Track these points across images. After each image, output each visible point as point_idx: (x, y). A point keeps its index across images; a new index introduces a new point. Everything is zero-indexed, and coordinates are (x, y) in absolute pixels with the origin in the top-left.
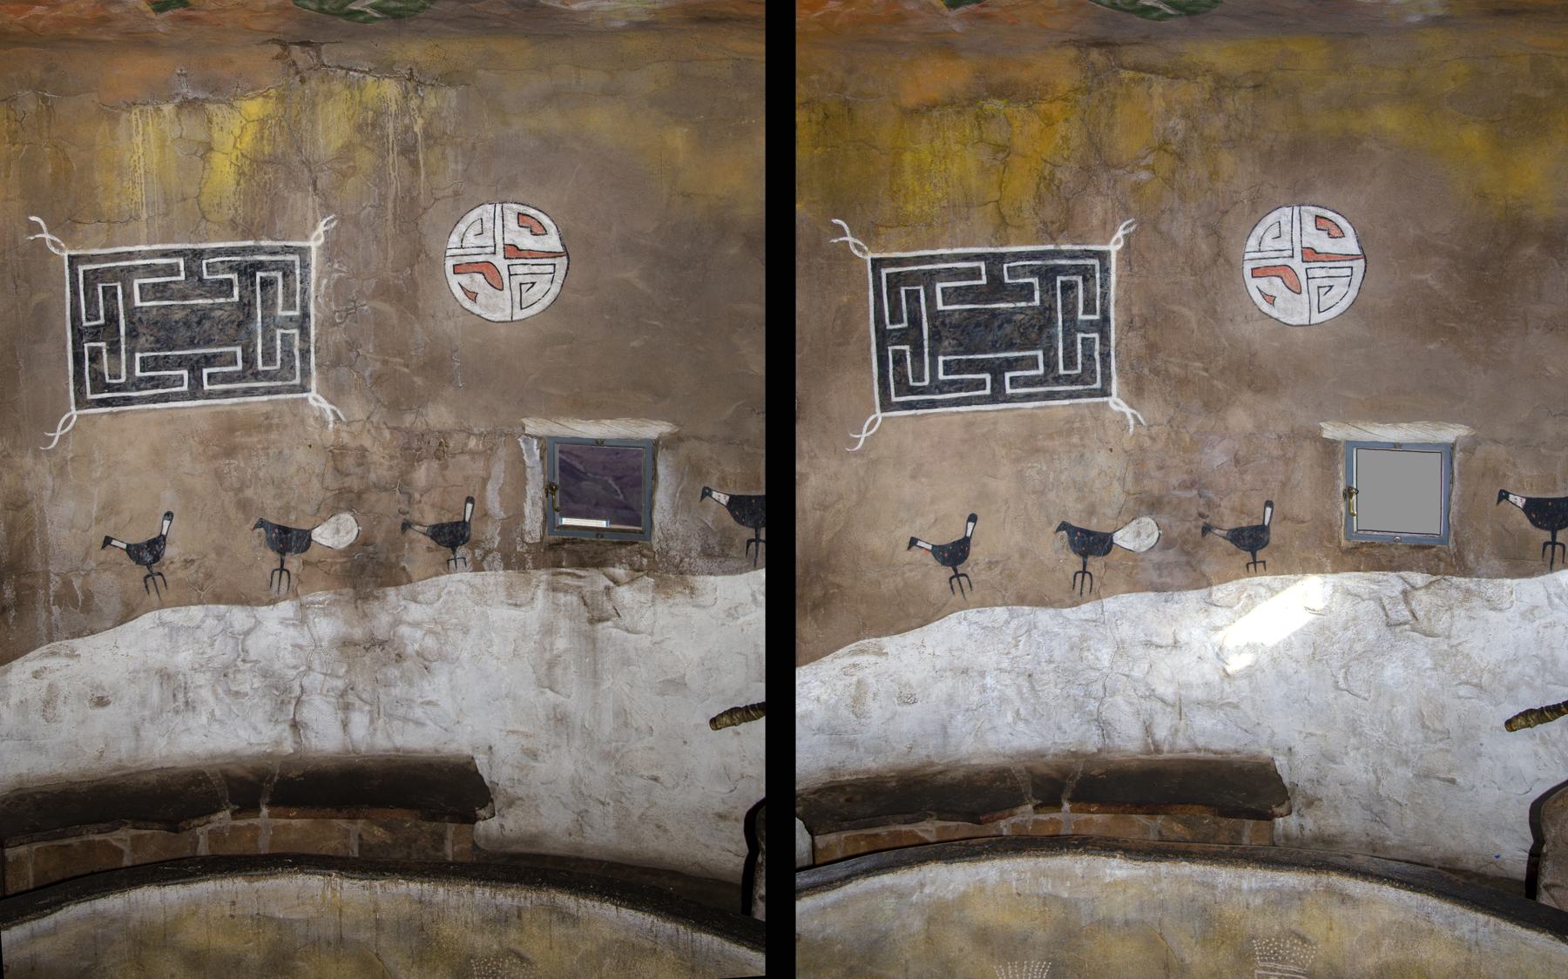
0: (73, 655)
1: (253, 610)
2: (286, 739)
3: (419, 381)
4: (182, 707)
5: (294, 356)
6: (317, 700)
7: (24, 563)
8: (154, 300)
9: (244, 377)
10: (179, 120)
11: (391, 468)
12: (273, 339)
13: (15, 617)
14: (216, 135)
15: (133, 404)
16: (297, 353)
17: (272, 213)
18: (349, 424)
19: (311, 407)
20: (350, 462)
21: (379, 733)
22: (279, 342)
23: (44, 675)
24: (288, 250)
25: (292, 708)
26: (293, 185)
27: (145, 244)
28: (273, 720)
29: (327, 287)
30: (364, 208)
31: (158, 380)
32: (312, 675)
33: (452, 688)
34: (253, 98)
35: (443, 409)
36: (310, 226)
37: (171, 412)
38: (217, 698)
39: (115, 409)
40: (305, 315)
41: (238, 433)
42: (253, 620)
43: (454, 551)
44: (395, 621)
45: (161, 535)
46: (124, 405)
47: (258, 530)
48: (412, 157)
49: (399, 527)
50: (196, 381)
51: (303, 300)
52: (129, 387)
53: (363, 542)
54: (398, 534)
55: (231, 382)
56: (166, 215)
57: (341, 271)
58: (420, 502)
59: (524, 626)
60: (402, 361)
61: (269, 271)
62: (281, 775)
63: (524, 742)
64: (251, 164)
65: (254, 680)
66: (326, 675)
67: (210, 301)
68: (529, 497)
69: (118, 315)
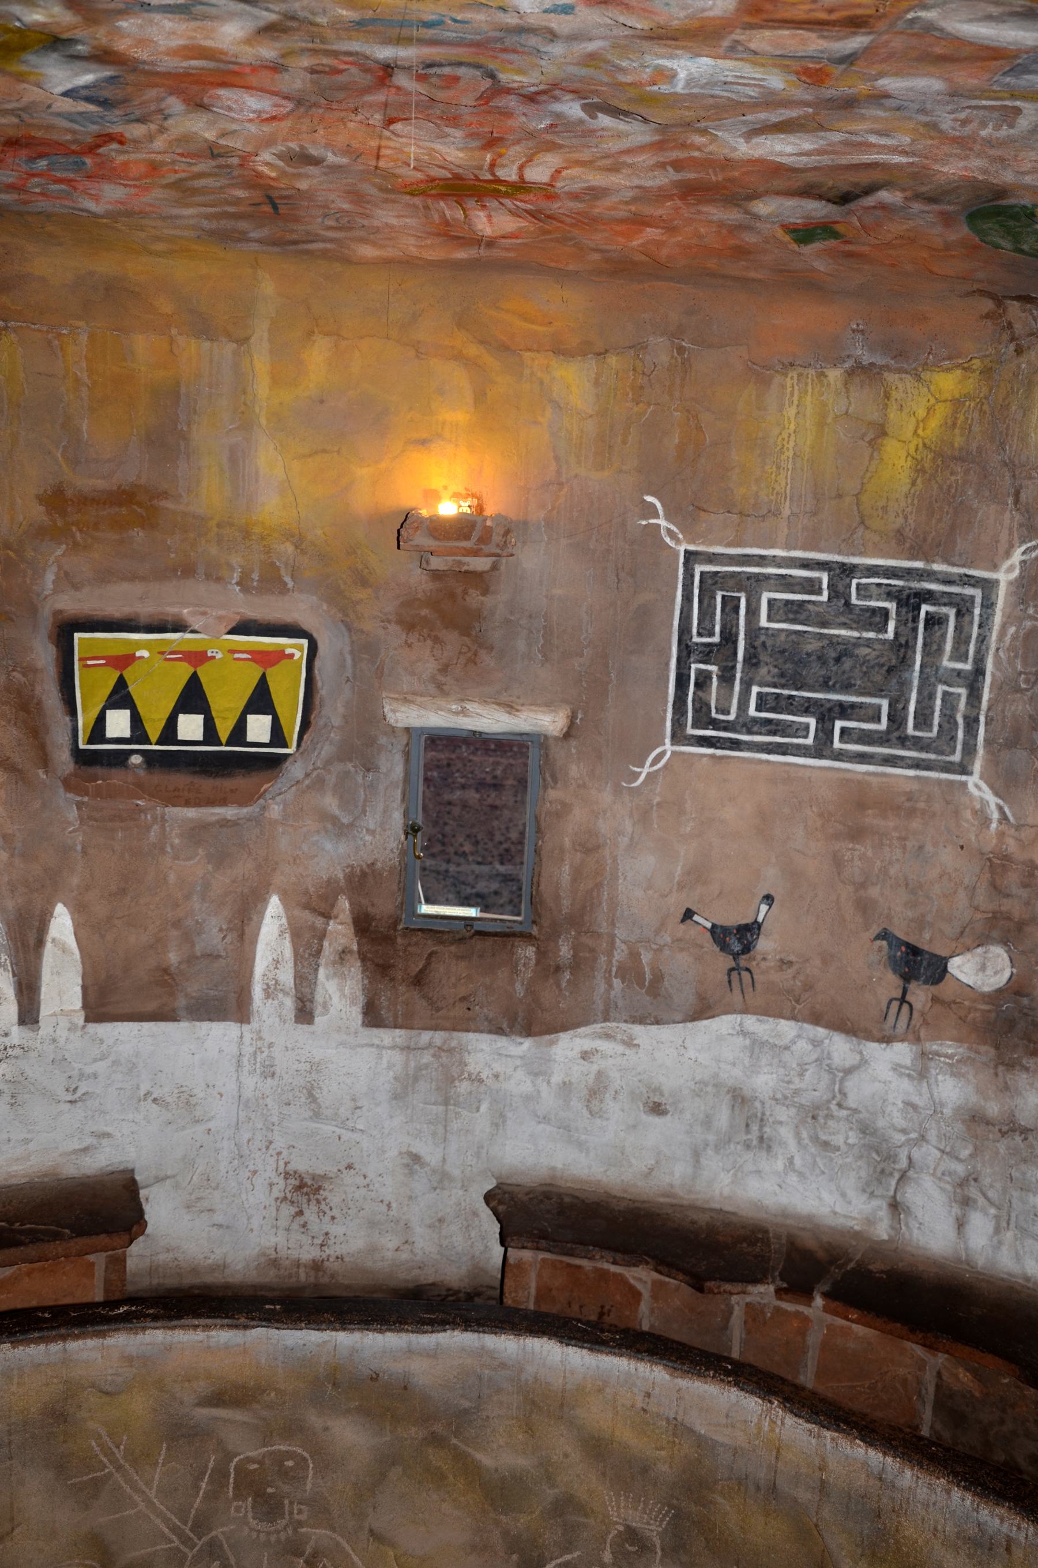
0: (630, 1043)
1: (859, 1044)
2: (881, 1220)
4: (755, 1143)
5: (956, 723)
6: (928, 1183)
7: (586, 918)
9: (888, 741)
10: (847, 391)
12: (932, 696)
13: (569, 981)
14: (893, 415)
15: (741, 750)
16: (960, 720)
18: (1018, 828)
21: (1005, 1249)
22: (938, 702)
23: (594, 1059)
24: (967, 580)
25: (893, 1182)
26: (987, 494)
27: (783, 548)
28: (867, 1190)
29: (1014, 638)
31: (777, 725)
32: (925, 1148)
34: (948, 370)
36: (1001, 551)
37: (787, 768)
38: (799, 1143)
39: (719, 752)
40: (979, 671)
41: (870, 812)
42: (858, 1057)
45: (756, 921)
47: (878, 943)
50: (825, 734)
51: (978, 651)
52: (738, 728)
53: (1015, 989)
55: (869, 744)
61: (940, 605)
62: (859, 1264)
64: (934, 459)
65: (850, 1134)
66: (943, 1152)
67: (856, 634)
69: (737, 635)
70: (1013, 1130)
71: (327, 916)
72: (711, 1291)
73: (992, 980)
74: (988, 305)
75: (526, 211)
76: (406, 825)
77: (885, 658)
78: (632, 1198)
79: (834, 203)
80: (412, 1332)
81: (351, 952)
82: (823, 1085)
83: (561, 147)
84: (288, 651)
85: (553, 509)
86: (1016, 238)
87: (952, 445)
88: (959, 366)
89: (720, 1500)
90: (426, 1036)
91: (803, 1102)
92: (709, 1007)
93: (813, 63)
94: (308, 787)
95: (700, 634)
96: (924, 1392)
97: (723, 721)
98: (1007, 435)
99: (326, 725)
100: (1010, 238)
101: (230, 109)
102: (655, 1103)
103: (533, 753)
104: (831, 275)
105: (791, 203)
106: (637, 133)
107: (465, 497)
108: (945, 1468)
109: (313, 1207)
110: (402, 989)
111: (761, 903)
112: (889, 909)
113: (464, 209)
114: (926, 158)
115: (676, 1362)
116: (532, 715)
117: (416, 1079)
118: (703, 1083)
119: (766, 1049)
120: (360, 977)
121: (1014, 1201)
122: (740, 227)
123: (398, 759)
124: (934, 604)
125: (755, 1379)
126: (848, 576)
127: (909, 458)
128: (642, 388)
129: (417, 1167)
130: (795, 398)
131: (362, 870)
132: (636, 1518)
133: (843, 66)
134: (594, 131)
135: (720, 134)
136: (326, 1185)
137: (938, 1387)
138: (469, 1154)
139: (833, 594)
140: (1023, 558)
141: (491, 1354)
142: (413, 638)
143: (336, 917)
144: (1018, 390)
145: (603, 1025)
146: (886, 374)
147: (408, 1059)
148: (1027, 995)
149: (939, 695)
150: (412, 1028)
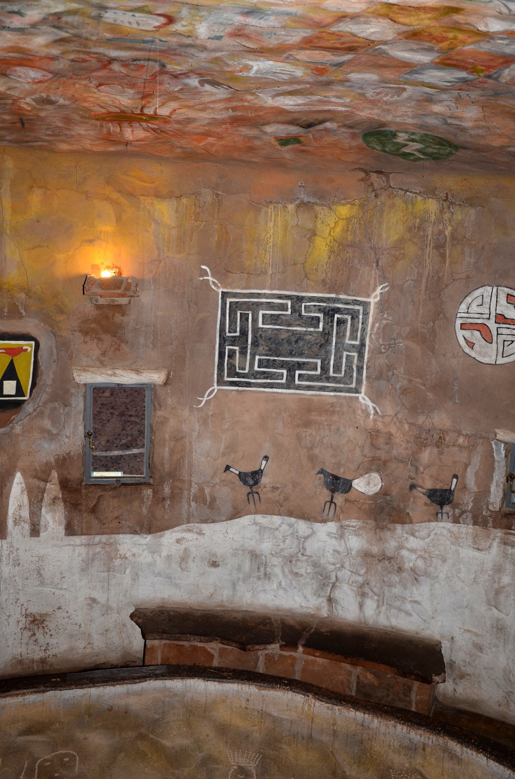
0: (200, 533)
2: (324, 607)
3: (430, 395)
4: (262, 576)
5: (353, 369)
6: (345, 587)
7: (177, 473)
8: (270, 324)
9: (321, 379)
10: (297, 214)
11: (406, 448)
12: (341, 357)
13: (169, 505)
16: (355, 368)
17: (348, 278)
19: (360, 403)
20: (381, 441)
21: (382, 615)
22: (344, 360)
23: (183, 542)
25: (329, 589)
26: (364, 262)
29: (378, 329)
30: (407, 281)
31: (268, 374)
32: (344, 571)
33: (432, 595)
34: (344, 205)
35: (444, 416)
36: (371, 288)
37: (274, 395)
38: (284, 574)
39: (241, 389)
40: (363, 345)
41: (313, 413)
42: (311, 531)
43: (442, 508)
44: (400, 546)
45: (260, 469)
46: (246, 387)
47: (319, 475)
48: (442, 251)
49: (408, 487)
50: (291, 377)
51: (362, 335)
53: (384, 493)
54: (407, 491)
55: (312, 381)
56: (284, 273)
57: (388, 320)
58: (423, 473)
59: (483, 564)
60: (421, 381)
61: (343, 314)
63: (474, 638)
65: (308, 568)
66: (352, 572)
67: (305, 329)
68: (495, 480)
69: (248, 331)
70: (384, 559)
71: (46, 481)
72: (249, 650)
73: (373, 489)
74: (362, 175)
75: (152, 129)
76: (85, 432)
77: (319, 340)
78: (203, 609)
79: (303, 127)
80: (129, 684)
81: (58, 498)
82: (294, 545)
83: (180, 99)
84: (25, 348)
85: (156, 273)
86: (383, 145)
87: (347, 239)
88: (349, 203)
89: (284, 746)
90: (97, 538)
91: (285, 554)
92: (239, 512)
93: (321, 65)
94: (35, 416)
95: (230, 332)
96: (351, 686)
97: (242, 373)
98: (372, 235)
99: (44, 384)
100: (381, 145)
101: (20, 77)
102: (213, 561)
103: (147, 393)
104: (292, 161)
105: (282, 127)
106: (221, 93)
107: (112, 268)
108: (393, 716)
109: (41, 631)
110: (85, 515)
111: (263, 460)
112: (324, 459)
113: (120, 127)
114: (355, 108)
115: (260, 683)
116: (149, 374)
117: (93, 560)
118: (236, 549)
119: (267, 530)
120: (63, 511)
121: (386, 592)
122: (255, 138)
123: (81, 399)
124: (341, 314)
125: (299, 686)
126: (300, 302)
127: (327, 246)
128: (199, 213)
129: (94, 605)
130: (273, 218)
131: (63, 457)
132: (243, 762)
133: (336, 68)
134: (201, 92)
135: (261, 95)
136: (47, 619)
137: (358, 683)
138: (120, 595)
139: (293, 311)
140: (381, 291)
141: (169, 690)
142: (87, 339)
143: (51, 481)
144: (377, 214)
145: (187, 525)
146: (315, 207)
147: (89, 551)
148: (389, 495)
149: (344, 357)
150: (90, 535)
